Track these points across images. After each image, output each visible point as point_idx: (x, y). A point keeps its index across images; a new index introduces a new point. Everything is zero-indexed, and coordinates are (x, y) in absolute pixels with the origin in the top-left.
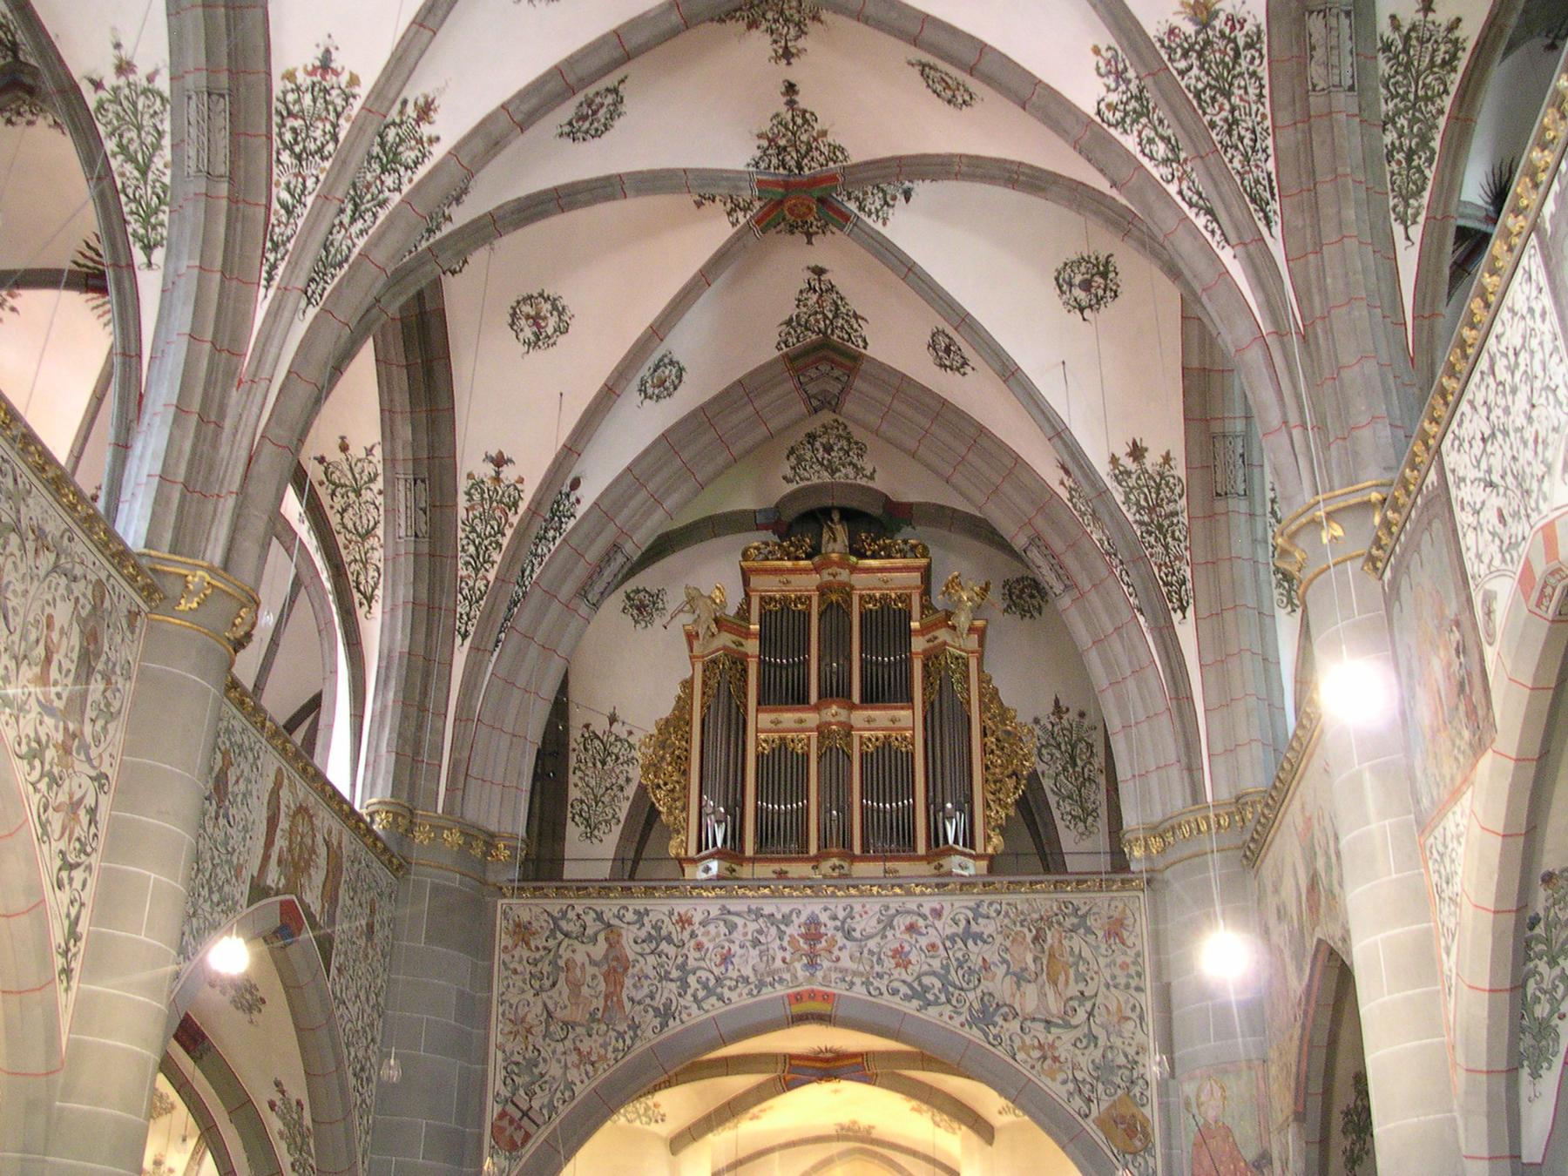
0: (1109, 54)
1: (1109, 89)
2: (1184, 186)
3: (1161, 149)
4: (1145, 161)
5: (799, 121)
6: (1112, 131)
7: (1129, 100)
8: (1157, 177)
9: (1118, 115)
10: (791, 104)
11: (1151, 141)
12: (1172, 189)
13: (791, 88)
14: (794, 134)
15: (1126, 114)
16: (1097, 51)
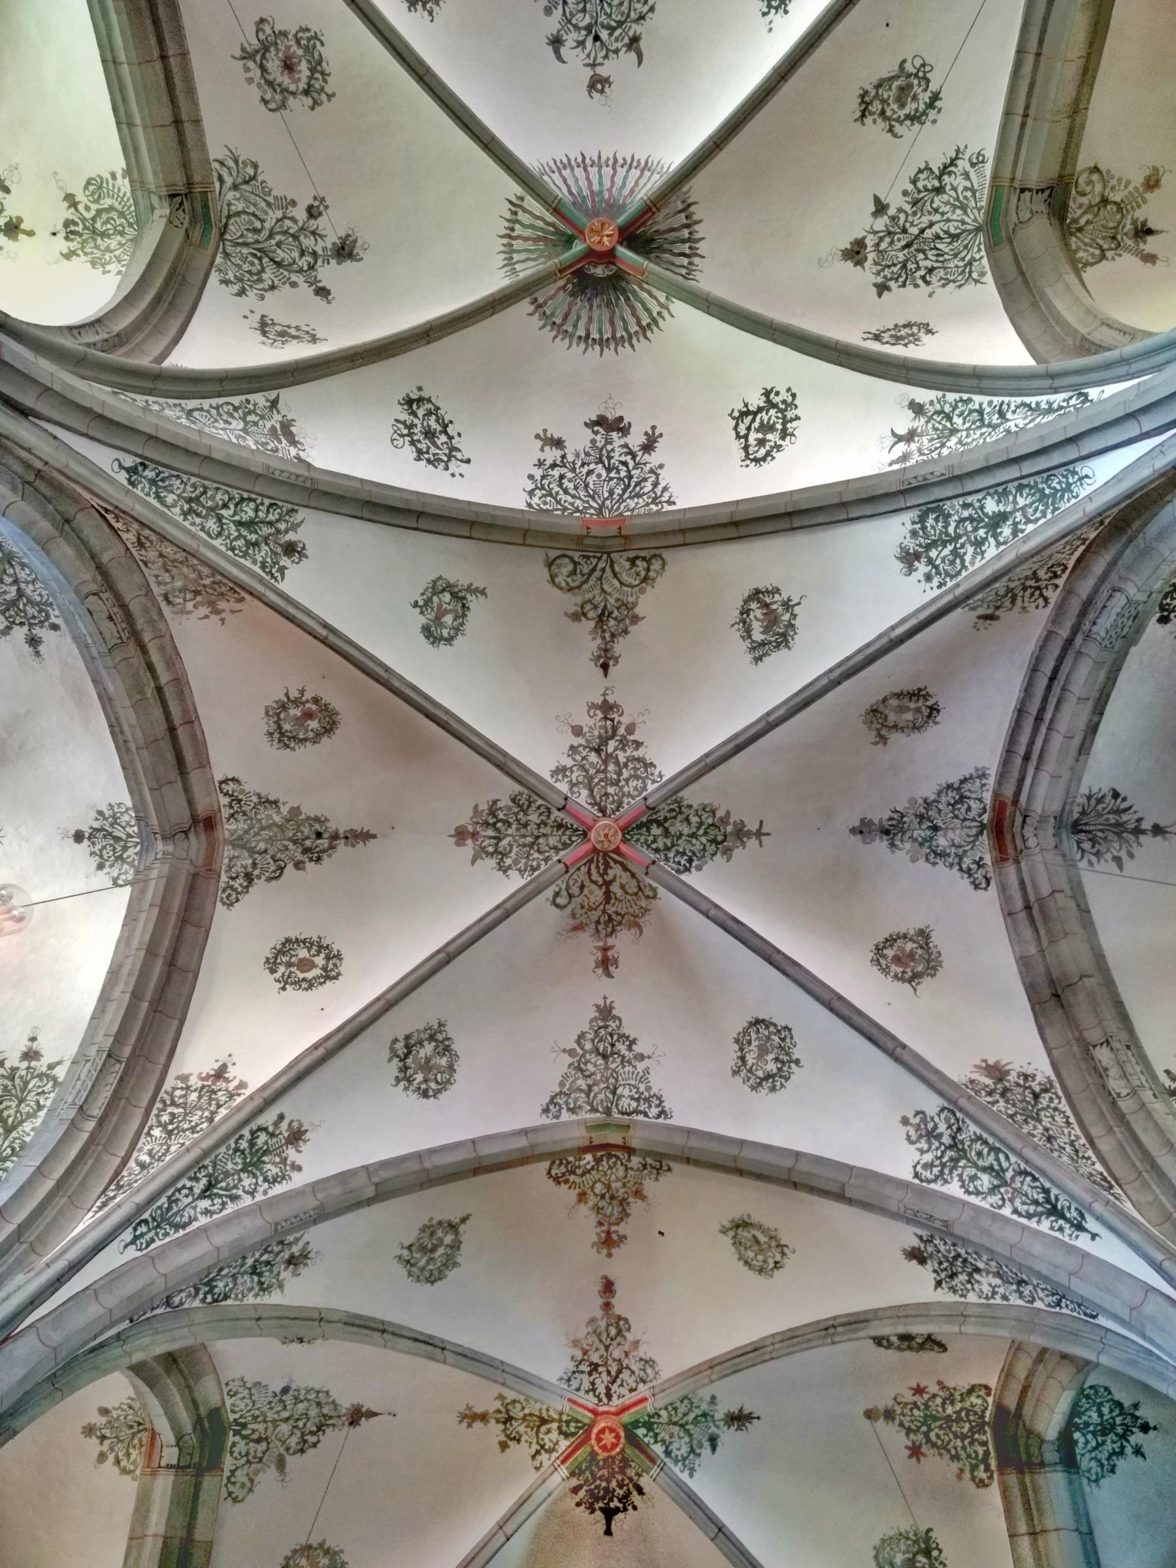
0: (917, 1120)
1: (922, 1152)
2: (1018, 1203)
3: (985, 1181)
4: (972, 1199)
5: (613, 1331)
6: (932, 1186)
7: (943, 1153)
8: (988, 1207)
9: (936, 1170)
10: (607, 1306)
11: (973, 1178)
12: (1007, 1211)
13: (608, 1287)
14: (607, 1348)
15: (943, 1165)
16: (905, 1121)
